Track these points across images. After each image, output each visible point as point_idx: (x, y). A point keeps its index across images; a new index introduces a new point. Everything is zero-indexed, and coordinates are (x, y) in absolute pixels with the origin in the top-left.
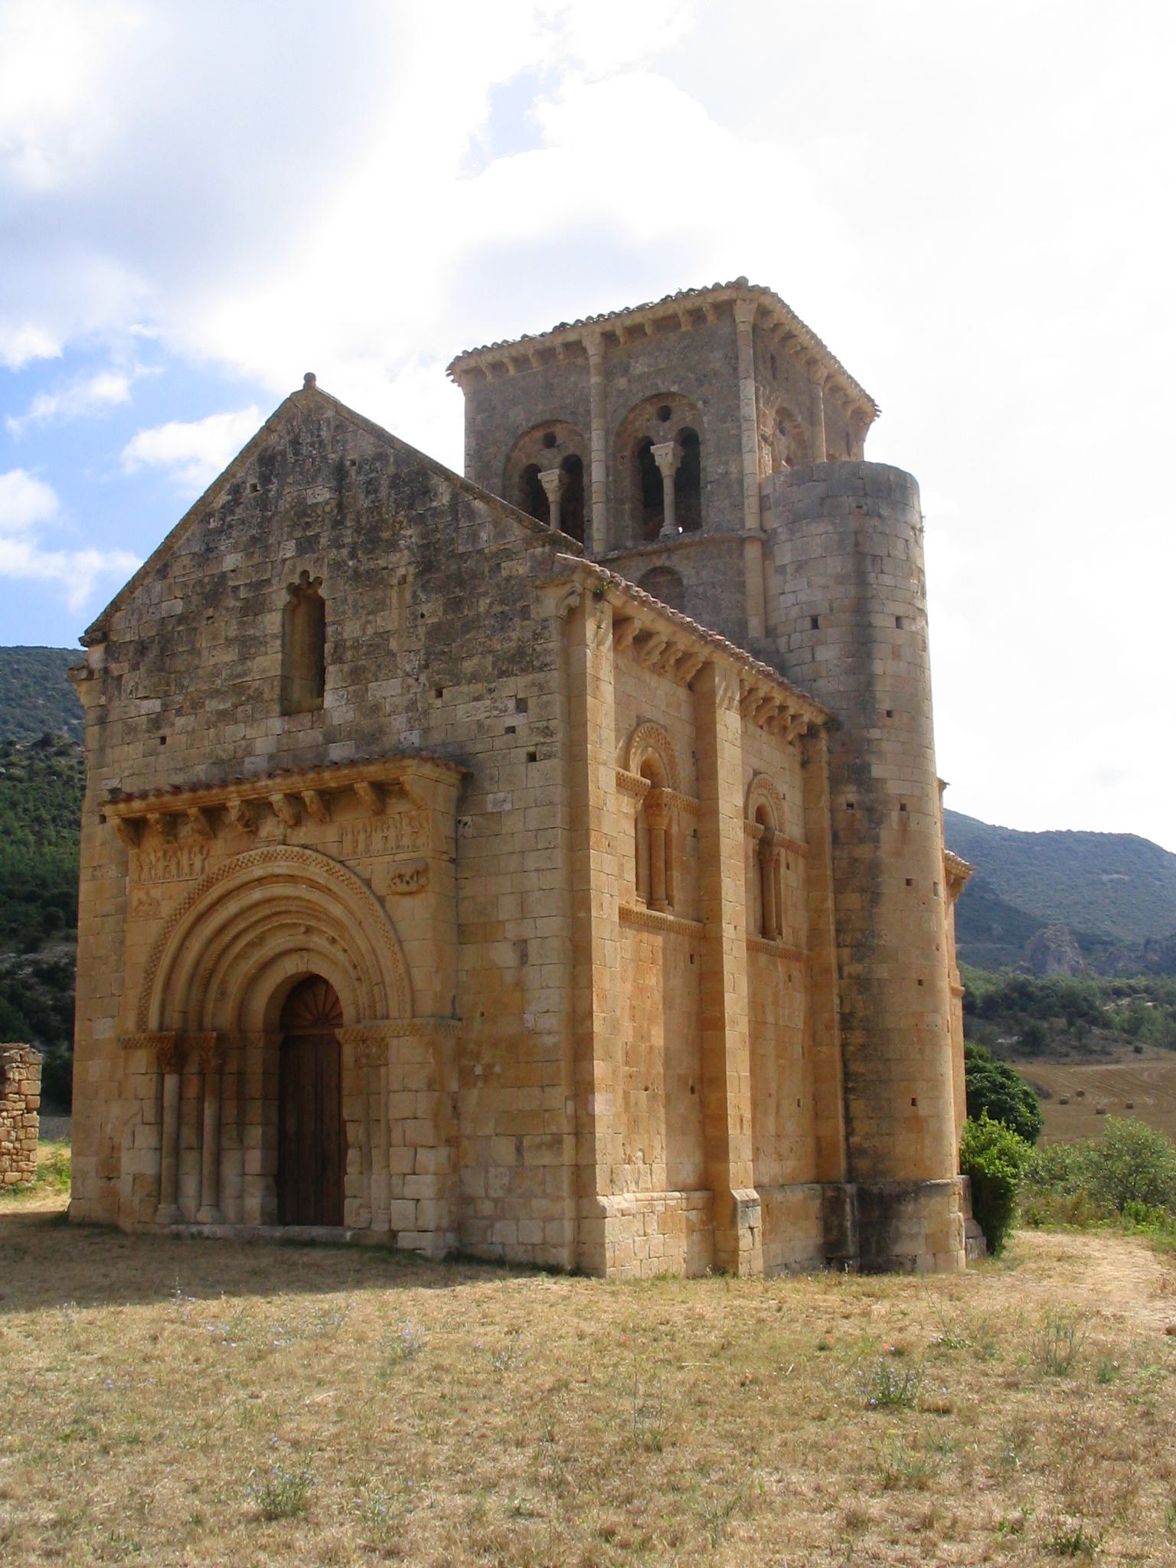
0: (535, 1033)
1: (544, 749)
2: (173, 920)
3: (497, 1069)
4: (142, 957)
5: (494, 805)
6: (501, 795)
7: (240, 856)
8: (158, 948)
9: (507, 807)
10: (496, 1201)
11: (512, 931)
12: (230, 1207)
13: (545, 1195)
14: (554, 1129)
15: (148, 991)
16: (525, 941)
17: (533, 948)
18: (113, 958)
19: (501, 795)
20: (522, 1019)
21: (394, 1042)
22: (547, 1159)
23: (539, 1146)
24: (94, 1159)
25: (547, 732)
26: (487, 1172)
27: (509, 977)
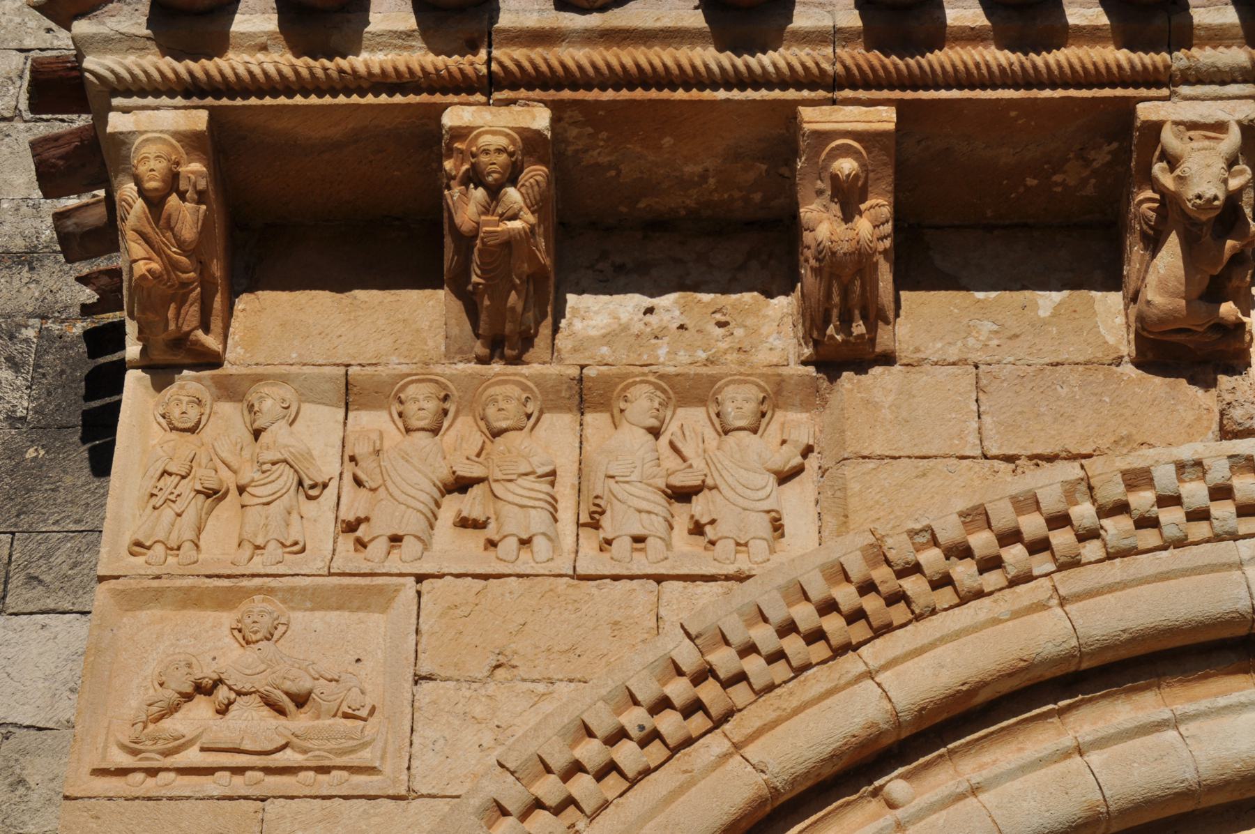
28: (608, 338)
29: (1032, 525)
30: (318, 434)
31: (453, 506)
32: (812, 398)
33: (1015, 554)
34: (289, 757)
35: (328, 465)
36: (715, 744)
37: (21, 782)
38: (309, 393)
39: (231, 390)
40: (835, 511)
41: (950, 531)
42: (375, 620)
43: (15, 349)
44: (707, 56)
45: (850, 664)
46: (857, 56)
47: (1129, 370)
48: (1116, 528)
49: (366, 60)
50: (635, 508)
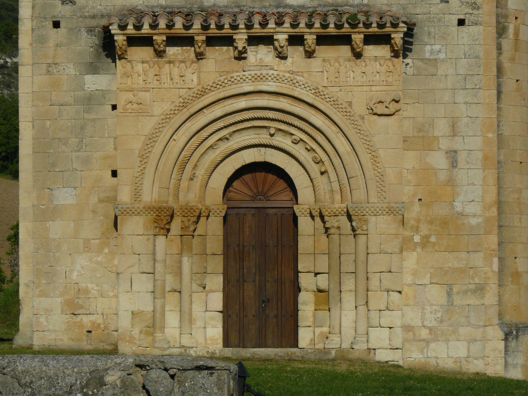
0: (462, 214)
1: (472, 18)
2: (167, 118)
3: (433, 239)
4: (137, 145)
5: (432, 53)
6: (437, 47)
7: (235, 75)
8: (152, 139)
9: (442, 56)
10: (431, 329)
11: (444, 144)
12: (198, 335)
13: (469, 324)
14: (477, 280)
15: (142, 173)
16: (455, 152)
17: (462, 157)
18: (73, 141)
19: (437, 47)
20: (452, 206)
21: (373, 219)
22: (472, 300)
23: (465, 292)
24: (59, 300)
25: (475, 6)
26: (423, 309)
27: (443, 176)
28: (173, 55)
29: (220, 83)
30: (139, 67)
31: (156, 77)
32: (196, 62)
33: (218, 86)
34: (140, 111)
35: (141, 72)
36: (185, 110)
37: (105, 97)
38: (138, 62)
39: (129, 62)
40: (199, 78)
41: (211, 85)
42: (148, 94)
43: (95, 33)
44: (183, 31)
45: (200, 100)
46: (201, 31)
47: (233, 59)
48: (229, 83)
49: (143, 31)
50: (177, 79)
